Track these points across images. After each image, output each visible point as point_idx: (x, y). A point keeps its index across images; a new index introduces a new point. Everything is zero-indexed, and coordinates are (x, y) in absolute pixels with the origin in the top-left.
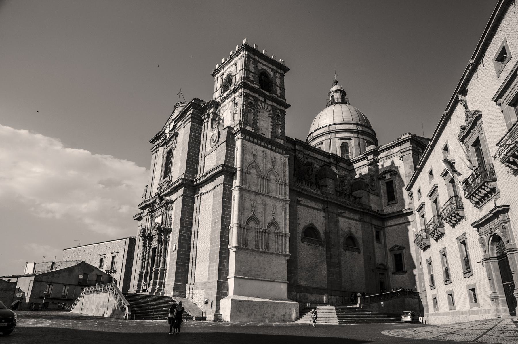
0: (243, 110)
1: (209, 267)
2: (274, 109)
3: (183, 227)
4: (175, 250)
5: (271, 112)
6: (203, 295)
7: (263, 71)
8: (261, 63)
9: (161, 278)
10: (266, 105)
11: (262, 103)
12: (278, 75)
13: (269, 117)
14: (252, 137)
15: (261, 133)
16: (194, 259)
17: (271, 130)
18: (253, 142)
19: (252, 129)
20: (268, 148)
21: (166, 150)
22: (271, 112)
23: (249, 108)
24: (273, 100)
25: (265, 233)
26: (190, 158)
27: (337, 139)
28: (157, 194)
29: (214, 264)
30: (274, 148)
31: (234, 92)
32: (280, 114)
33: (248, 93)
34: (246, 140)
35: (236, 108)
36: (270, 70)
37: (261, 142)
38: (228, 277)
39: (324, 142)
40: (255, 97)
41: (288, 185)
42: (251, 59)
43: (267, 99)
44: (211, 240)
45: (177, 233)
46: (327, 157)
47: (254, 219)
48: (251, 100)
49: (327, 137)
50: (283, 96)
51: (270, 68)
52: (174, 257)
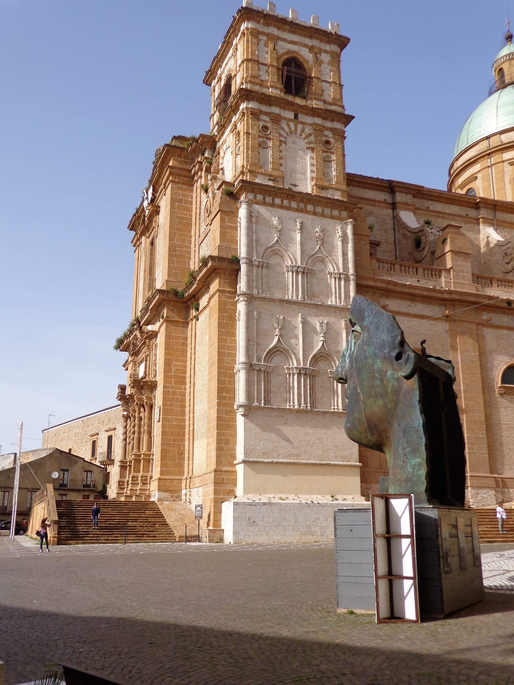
0: (247, 143)
2: (319, 130)
3: (170, 377)
4: (159, 419)
5: (312, 138)
7: (290, 55)
8: (284, 40)
9: (146, 470)
10: (300, 127)
11: (291, 123)
12: (325, 58)
13: (308, 148)
14: (269, 195)
15: (291, 184)
16: (191, 433)
17: (314, 175)
18: (273, 205)
19: (269, 180)
20: (307, 212)
21: (149, 240)
22: (312, 138)
23: (261, 139)
24: (314, 112)
25: (305, 374)
26: (175, 251)
27: (506, 164)
28: (135, 323)
30: (319, 209)
31: (233, 111)
32: (333, 138)
33: (257, 109)
34: (257, 203)
35: (238, 143)
36: (307, 50)
37: (290, 203)
38: (235, 462)
39: (479, 175)
40: (274, 113)
41: (352, 277)
42: (261, 37)
43: (302, 112)
46: (472, 207)
47: (282, 352)
48: (265, 121)
49: (487, 162)
50: (338, 101)
51: (305, 46)
52: (159, 432)
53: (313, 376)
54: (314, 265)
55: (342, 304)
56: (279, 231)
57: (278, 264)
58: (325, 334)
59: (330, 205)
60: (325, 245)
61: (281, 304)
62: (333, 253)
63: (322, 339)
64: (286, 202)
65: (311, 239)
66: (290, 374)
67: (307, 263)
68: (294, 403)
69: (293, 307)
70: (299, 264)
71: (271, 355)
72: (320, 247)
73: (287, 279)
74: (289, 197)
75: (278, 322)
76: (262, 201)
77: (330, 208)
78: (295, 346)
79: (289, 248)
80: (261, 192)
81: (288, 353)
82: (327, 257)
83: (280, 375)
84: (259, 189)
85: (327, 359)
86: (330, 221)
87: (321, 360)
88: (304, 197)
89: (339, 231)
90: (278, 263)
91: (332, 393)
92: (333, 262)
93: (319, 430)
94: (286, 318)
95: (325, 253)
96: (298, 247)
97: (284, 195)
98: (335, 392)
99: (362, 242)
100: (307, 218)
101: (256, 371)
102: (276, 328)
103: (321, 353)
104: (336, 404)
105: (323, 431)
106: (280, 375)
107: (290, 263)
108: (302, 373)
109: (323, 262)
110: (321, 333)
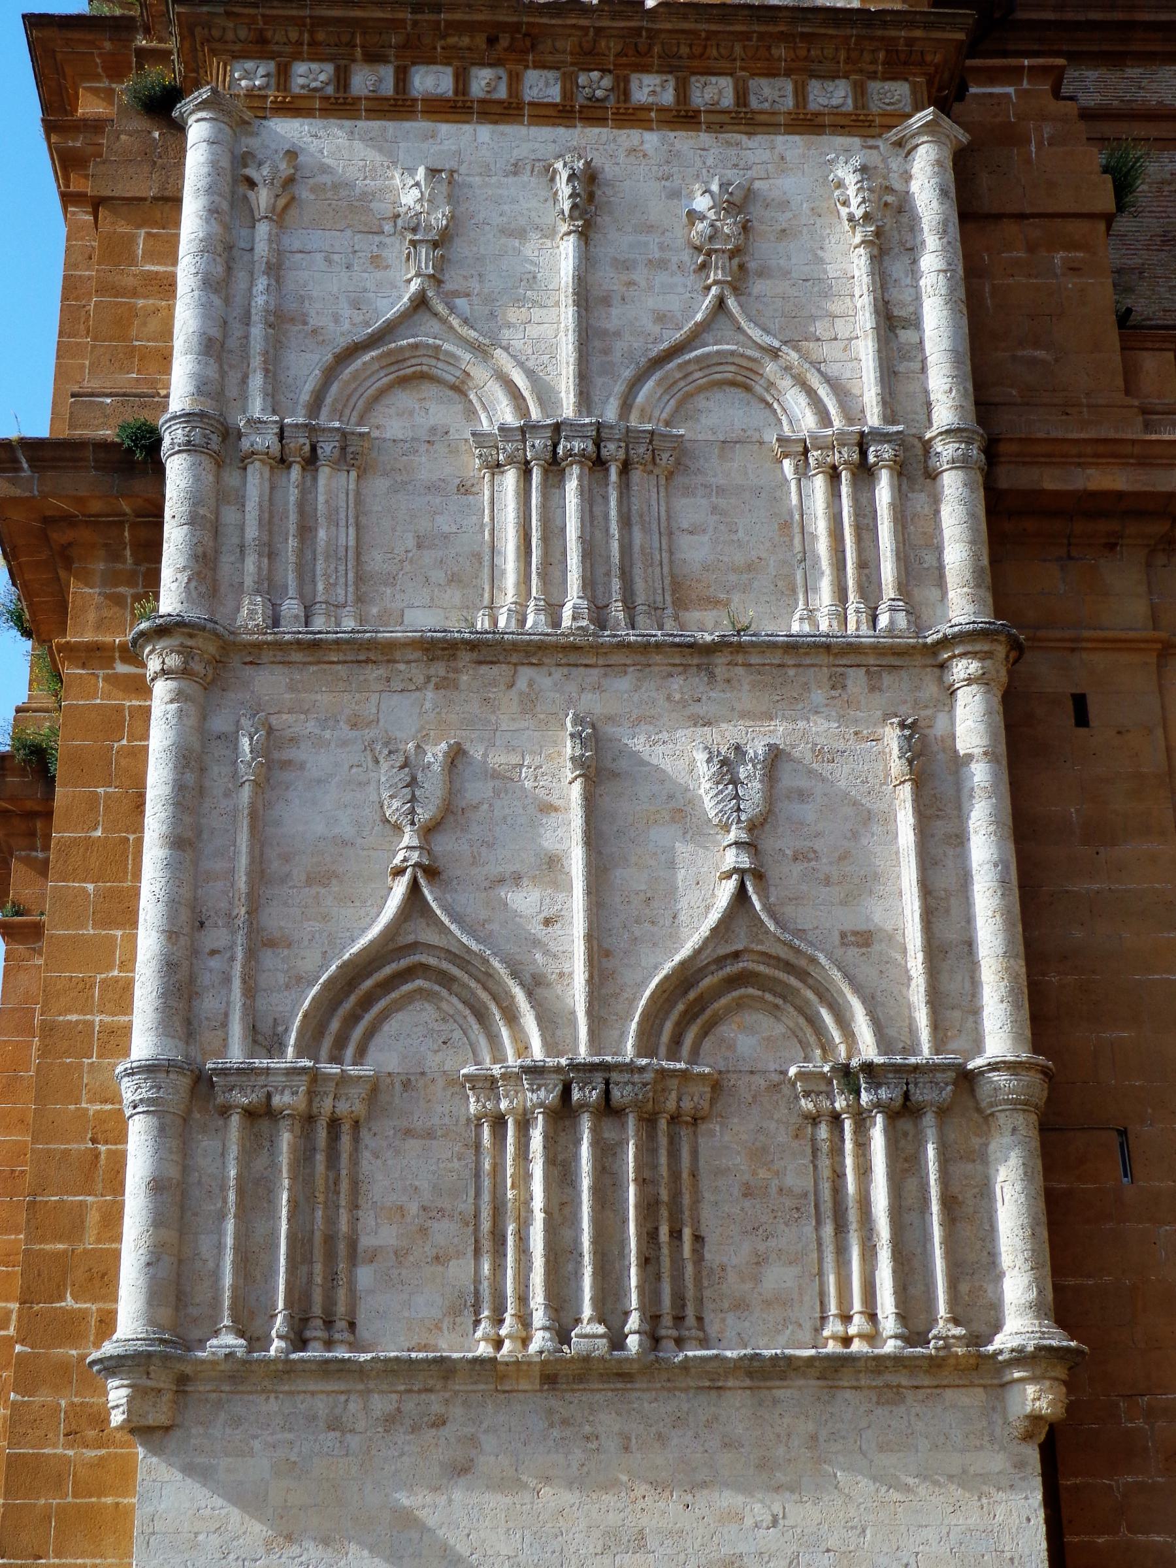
14: (374, 58)
25: (608, 1109)
34: (293, 108)
47: (446, 980)
53: (674, 1119)
54: (683, 410)
55: (883, 621)
56: (435, 245)
57: (436, 436)
58: (752, 827)
59: (780, 51)
60: (759, 287)
61: (439, 669)
62: (820, 328)
63: (731, 858)
64: (482, 80)
65: (661, 264)
66: (499, 1122)
67: (626, 406)
68: (525, 1320)
69: (522, 684)
70: (568, 407)
71: (367, 1002)
72: (721, 303)
73: (487, 519)
74: (504, 42)
75: (413, 783)
76: (330, 90)
77: (788, 73)
78: (536, 929)
79: (506, 334)
80: (313, 43)
81: (487, 978)
82: (774, 354)
83: (430, 1135)
84: (298, 22)
85: (786, 993)
86: (791, 145)
87: (739, 1005)
88: (599, 31)
89: (851, 191)
90: (433, 430)
91: (828, 1230)
92: (814, 381)
93: (728, 1499)
94: (476, 752)
95: (755, 333)
96: (567, 315)
97: (466, 41)
98: (853, 1216)
99: (1059, 257)
100: (632, 151)
101: (235, 1120)
102: (398, 829)
103: (736, 955)
104: (857, 1305)
105: (757, 1510)
106: (430, 1135)
107: (508, 416)
108: (583, 1105)
109: (748, 389)
110: (726, 828)
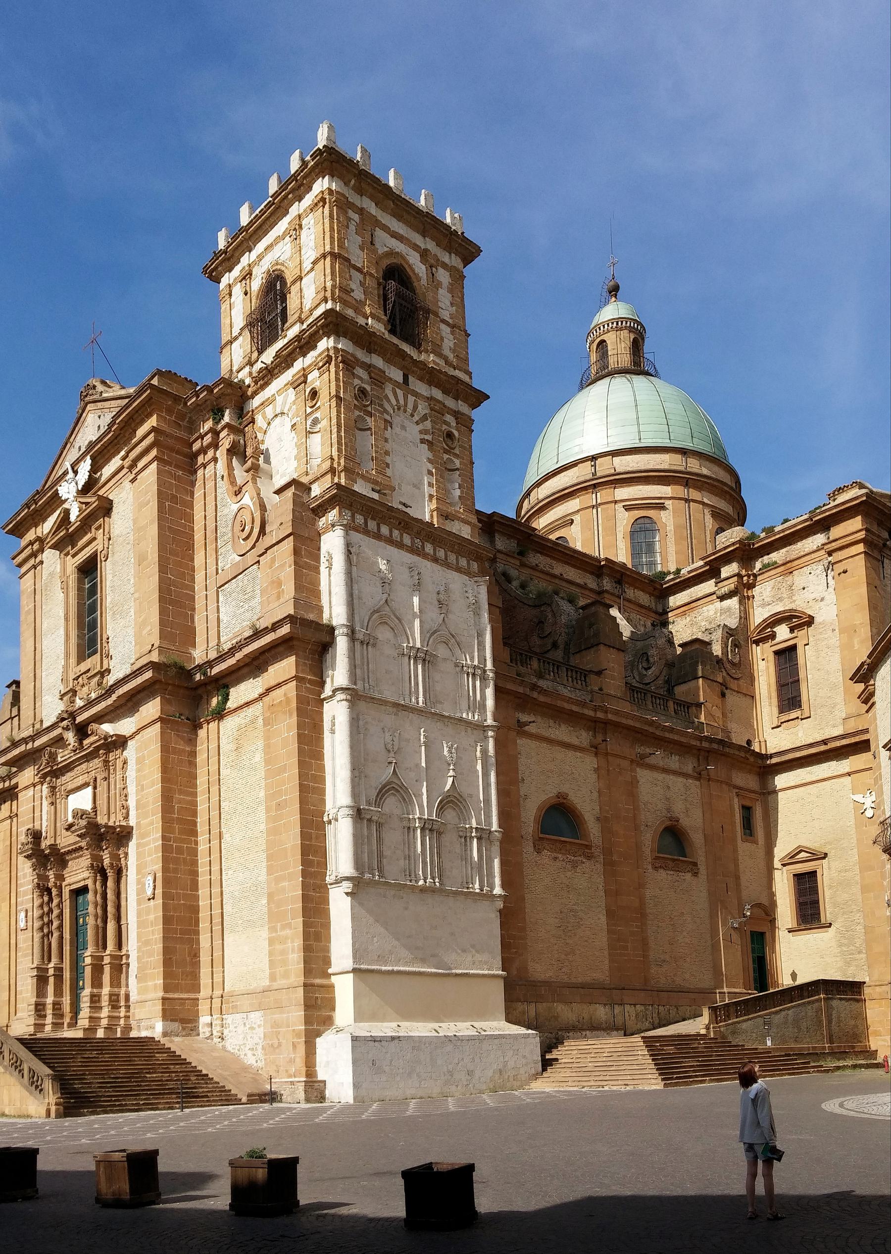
1: (271, 942)
6: (259, 1026)
29: (288, 932)
44: (269, 858)
45: (155, 840)
